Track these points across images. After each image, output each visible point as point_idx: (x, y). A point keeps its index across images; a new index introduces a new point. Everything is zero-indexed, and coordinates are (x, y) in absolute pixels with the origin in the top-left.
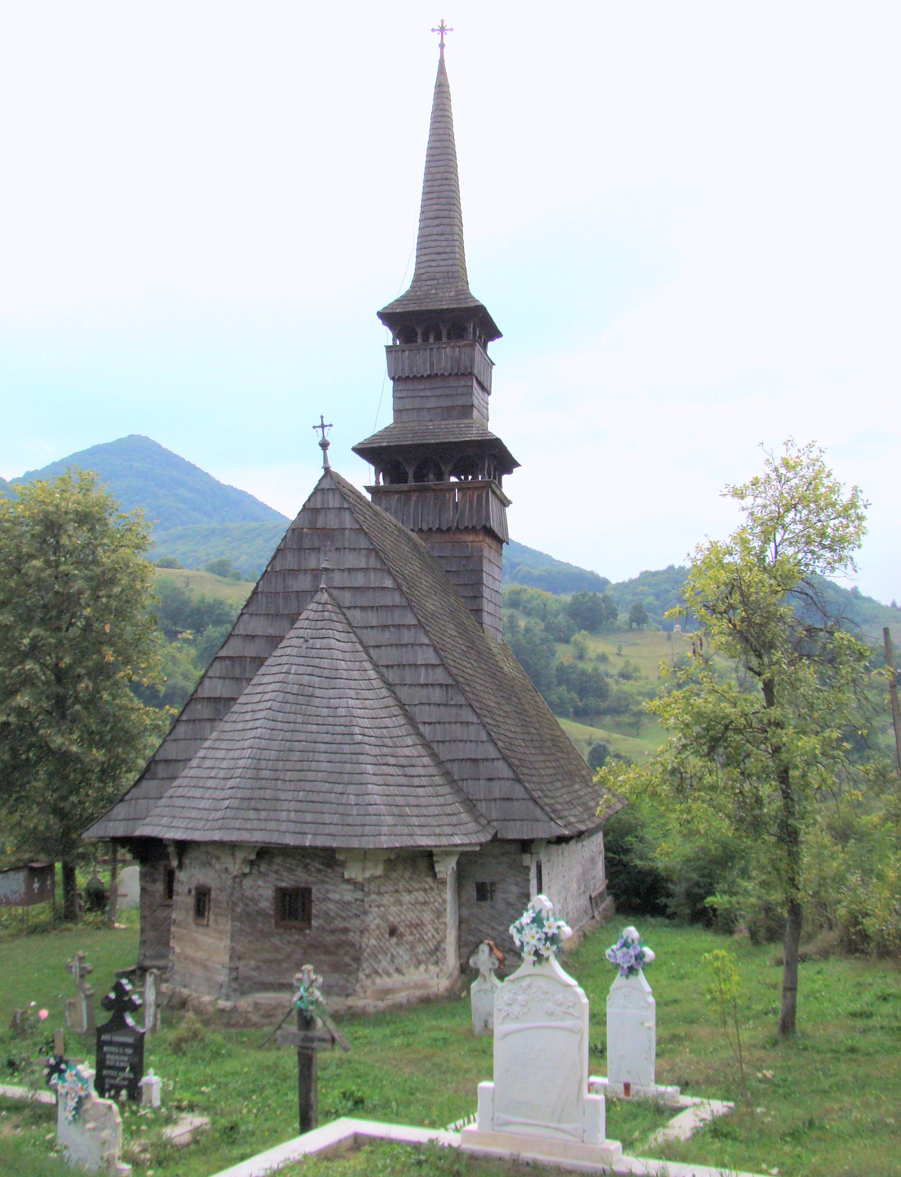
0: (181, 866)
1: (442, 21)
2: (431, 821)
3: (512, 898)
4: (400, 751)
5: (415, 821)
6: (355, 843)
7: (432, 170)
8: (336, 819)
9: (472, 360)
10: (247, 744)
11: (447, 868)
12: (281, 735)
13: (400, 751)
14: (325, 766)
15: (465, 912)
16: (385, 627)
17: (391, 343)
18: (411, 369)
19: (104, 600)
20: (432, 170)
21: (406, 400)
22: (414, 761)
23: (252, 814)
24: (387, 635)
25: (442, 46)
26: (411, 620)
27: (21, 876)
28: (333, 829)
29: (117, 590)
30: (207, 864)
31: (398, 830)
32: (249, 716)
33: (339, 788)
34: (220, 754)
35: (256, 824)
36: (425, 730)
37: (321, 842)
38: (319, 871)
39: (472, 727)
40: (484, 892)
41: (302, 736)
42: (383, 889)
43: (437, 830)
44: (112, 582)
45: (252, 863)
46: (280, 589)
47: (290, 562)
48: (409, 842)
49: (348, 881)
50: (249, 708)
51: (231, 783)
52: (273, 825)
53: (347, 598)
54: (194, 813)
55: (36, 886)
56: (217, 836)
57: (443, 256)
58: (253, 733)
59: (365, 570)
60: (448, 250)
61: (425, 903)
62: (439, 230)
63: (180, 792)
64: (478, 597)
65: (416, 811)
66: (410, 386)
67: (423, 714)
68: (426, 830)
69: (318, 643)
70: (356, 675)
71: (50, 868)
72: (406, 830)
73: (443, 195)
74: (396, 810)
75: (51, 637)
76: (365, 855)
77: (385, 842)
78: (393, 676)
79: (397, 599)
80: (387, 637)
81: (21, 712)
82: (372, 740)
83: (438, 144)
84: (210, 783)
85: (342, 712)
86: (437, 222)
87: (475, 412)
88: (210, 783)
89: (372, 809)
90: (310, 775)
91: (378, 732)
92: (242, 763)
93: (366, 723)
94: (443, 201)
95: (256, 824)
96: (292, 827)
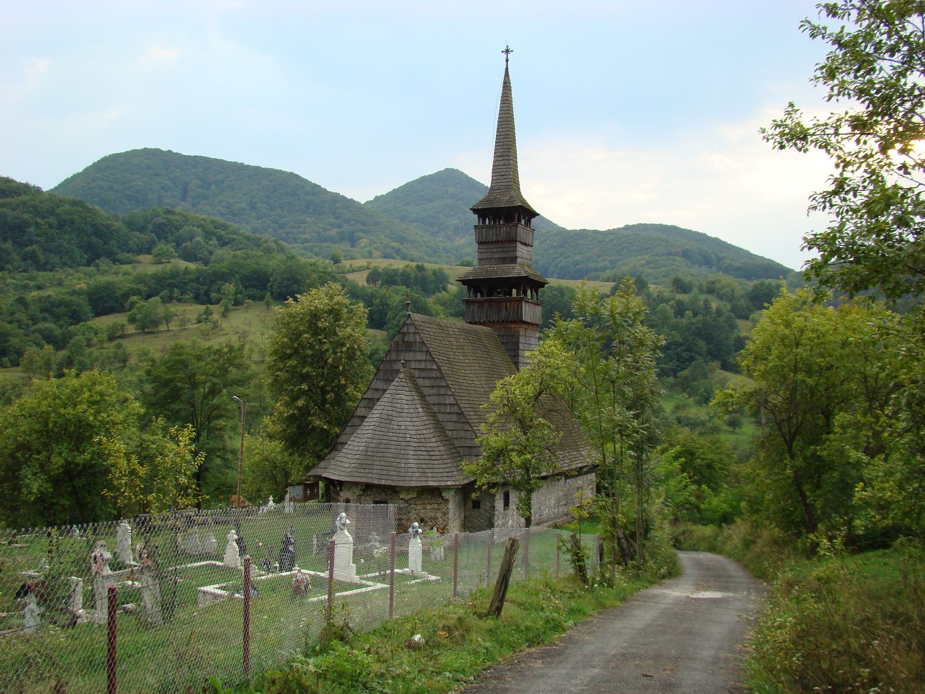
0: (341, 490)
1: (507, 47)
2: (438, 475)
3: (487, 508)
4: (428, 445)
5: (430, 475)
6: (401, 484)
7: (500, 130)
8: (395, 473)
9: (516, 234)
10: (364, 440)
11: (447, 495)
12: (377, 437)
13: (428, 445)
14: (394, 451)
15: (467, 513)
16: (433, 387)
17: (477, 224)
18: (486, 237)
19: (339, 354)
20: (500, 130)
21: (484, 254)
22: (434, 449)
23: (362, 471)
24: (434, 390)
25: (507, 61)
26: (444, 384)
27: (301, 487)
28: (393, 478)
29: (345, 349)
30: (349, 490)
31: (420, 479)
32: (367, 428)
33: (398, 460)
34: (355, 444)
35: (363, 475)
36: (449, 433)
37: (388, 483)
38: (391, 494)
39: (469, 433)
40: (477, 504)
41: (385, 438)
42: (418, 503)
43: (440, 479)
44: (343, 345)
45: (364, 490)
46: (389, 368)
47: (393, 356)
48: (425, 484)
49: (402, 499)
50: (367, 424)
51: (357, 457)
52: (370, 475)
53: (417, 373)
54: (342, 469)
55: (308, 492)
56: (347, 479)
57: (504, 177)
58: (367, 436)
59: (425, 361)
60: (507, 173)
61: (438, 509)
62: (502, 163)
63: (340, 459)
64: (517, 356)
65: (431, 470)
66: (486, 246)
67: (449, 426)
68: (434, 479)
69: (397, 397)
70: (412, 411)
71: (317, 484)
72: (424, 479)
73: (506, 143)
74: (421, 470)
75: (315, 371)
76: (409, 489)
77: (413, 484)
78: (436, 409)
79: (439, 375)
80: (434, 391)
81: (300, 409)
82: (415, 440)
83: (503, 116)
84: (350, 456)
85: (403, 427)
86: (501, 158)
87: (519, 260)
88: (350, 456)
89: (410, 470)
90: (387, 455)
91: (418, 436)
92: (361, 448)
93: (413, 432)
94: (505, 147)
95: (363, 475)
96: (377, 476)
